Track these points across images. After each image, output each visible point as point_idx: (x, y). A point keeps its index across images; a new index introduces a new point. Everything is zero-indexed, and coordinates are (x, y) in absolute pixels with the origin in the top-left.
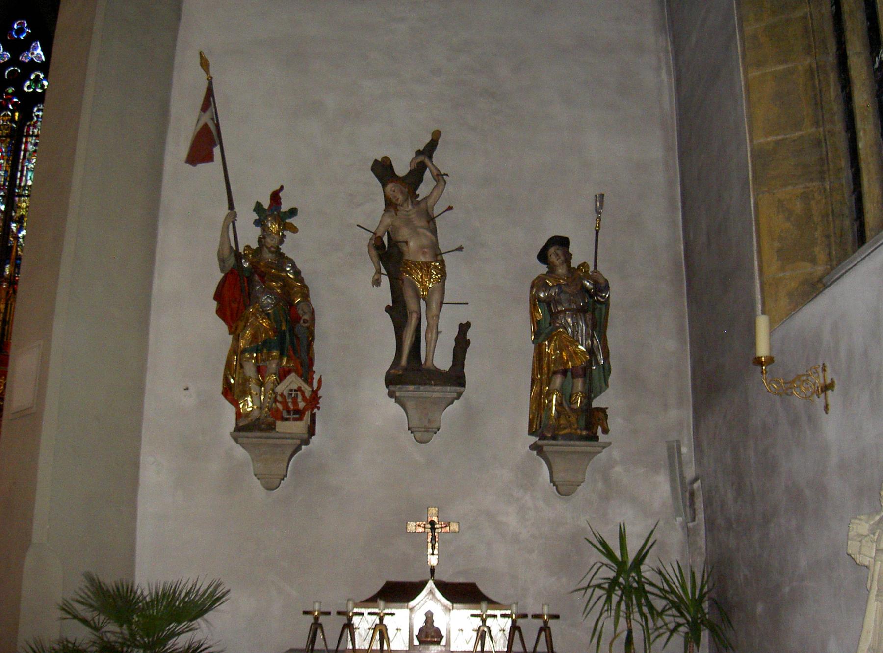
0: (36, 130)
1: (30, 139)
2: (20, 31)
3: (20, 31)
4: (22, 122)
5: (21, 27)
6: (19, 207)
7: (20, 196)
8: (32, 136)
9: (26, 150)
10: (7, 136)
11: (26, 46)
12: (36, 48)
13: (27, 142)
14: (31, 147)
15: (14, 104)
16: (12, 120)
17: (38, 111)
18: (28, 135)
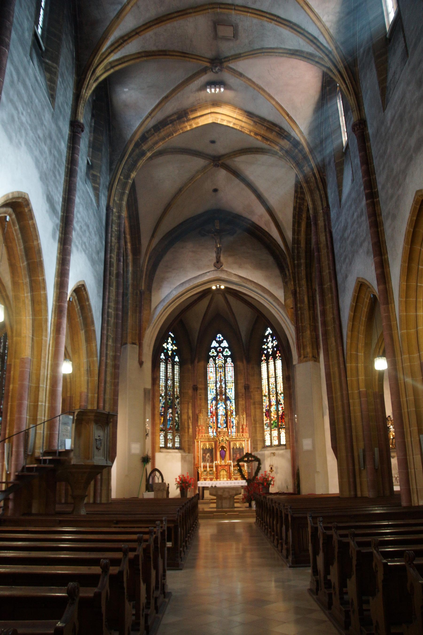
2: (219, 338)
3: (219, 338)
4: (225, 364)
5: (220, 336)
11: (221, 342)
14: (228, 370)
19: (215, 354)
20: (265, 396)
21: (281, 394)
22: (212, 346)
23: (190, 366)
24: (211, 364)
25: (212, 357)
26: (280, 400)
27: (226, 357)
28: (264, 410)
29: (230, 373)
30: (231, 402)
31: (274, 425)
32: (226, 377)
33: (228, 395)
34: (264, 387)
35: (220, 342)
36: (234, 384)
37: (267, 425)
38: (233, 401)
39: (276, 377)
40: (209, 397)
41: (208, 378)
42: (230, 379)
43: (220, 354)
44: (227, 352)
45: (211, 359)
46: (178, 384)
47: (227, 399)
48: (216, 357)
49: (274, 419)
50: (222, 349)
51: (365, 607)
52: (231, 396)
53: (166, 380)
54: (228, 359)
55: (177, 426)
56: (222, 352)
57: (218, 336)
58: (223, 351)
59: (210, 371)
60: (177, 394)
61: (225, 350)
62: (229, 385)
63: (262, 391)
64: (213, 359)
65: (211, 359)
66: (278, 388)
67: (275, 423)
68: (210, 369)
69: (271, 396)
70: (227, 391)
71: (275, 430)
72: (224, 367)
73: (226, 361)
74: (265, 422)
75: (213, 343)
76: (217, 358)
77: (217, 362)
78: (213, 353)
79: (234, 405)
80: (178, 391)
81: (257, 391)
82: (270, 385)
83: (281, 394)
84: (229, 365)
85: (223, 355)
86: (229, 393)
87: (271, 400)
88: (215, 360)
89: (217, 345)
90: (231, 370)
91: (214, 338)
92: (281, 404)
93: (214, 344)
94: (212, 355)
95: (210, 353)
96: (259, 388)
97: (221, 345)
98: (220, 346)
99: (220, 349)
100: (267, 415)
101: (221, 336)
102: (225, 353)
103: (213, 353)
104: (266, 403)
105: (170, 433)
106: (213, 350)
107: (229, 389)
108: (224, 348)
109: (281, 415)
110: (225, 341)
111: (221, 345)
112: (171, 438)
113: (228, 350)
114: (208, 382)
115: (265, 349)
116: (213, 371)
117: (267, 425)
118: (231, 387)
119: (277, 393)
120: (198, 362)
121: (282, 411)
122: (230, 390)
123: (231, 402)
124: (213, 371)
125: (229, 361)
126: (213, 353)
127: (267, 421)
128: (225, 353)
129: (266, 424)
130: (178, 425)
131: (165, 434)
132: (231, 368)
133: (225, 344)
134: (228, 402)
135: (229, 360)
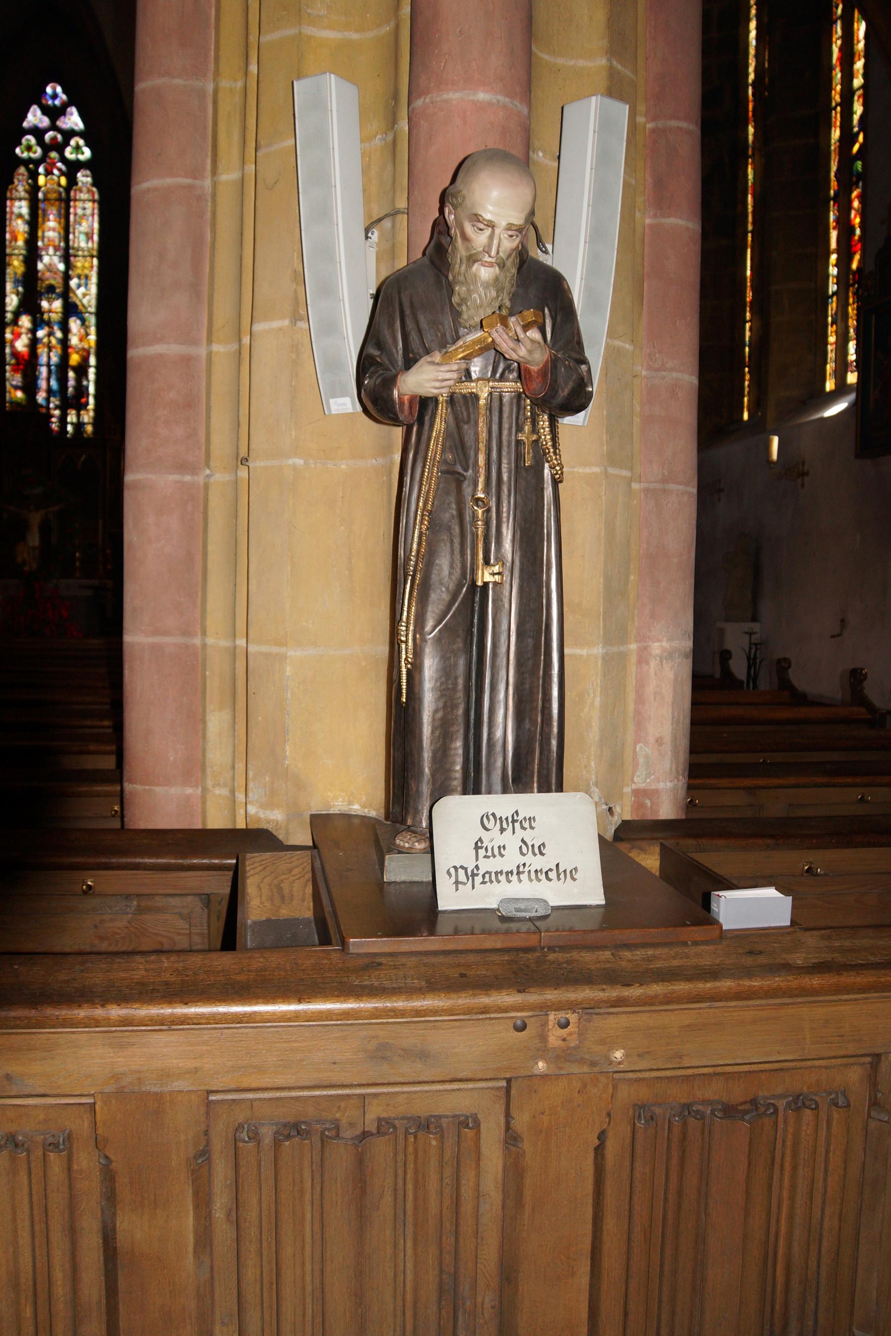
1: (77, 203)
3: (55, 96)
4: (68, 189)
5: (55, 91)
6: (75, 267)
7: (75, 256)
8: (80, 200)
9: (75, 214)
10: (56, 200)
12: (72, 114)
13: (75, 207)
14: (80, 212)
15: (60, 170)
16: (59, 185)
17: (83, 176)
18: (75, 200)
19: (38, 152)
22: (25, 124)
24: (20, 188)
25: (26, 162)
27: (73, 167)
29: (84, 224)
30: (83, 321)
32: (71, 236)
33: (73, 299)
35: (55, 113)
36: (95, 261)
38: (92, 320)
40: (8, 300)
41: (8, 236)
42: (83, 244)
43: (54, 155)
45: (22, 170)
47: (71, 309)
48: (37, 163)
50: (59, 137)
51: (502, 878)
52: (85, 301)
54: (79, 175)
56: (60, 148)
57: (49, 90)
58: (66, 143)
59: (16, 210)
61: (73, 142)
62: (79, 264)
64: (28, 169)
65: (22, 170)
68: (17, 204)
70: (73, 283)
72: (65, 201)
73: (72, 181)
75: (30, 116)
76: (41, 170)
77: (42, 180)
78: (28, 149)
79: (93, 330)
84: (84, 196)
85: (63, 160)
86: (80, 292)
88: (34, 175)
89: (45, 122)
90: (89, 212)
91: (37, 97)
93: (35, 117)
94: (25, 155)
95: (18, 151)
97: (60, 123)
98: (54, 127)
99: (54, 139)
101: (59, 89)
102: (69, 153)
103: (29, 148)
106: (31, 139)
107: (79, 277)
108: (69, 134)
110: (73, 110)
111: (60, 123)
113: (81, 142)
114: (8, 251)
118: (86, 272)
122: (83, 281)
123: (83, 321)
125: (85, 179)
126: (29, 148)
128: (69, 153)
132: (89, 205)
133: (74, 120)
134: (74, 324)
135: (84, 178)
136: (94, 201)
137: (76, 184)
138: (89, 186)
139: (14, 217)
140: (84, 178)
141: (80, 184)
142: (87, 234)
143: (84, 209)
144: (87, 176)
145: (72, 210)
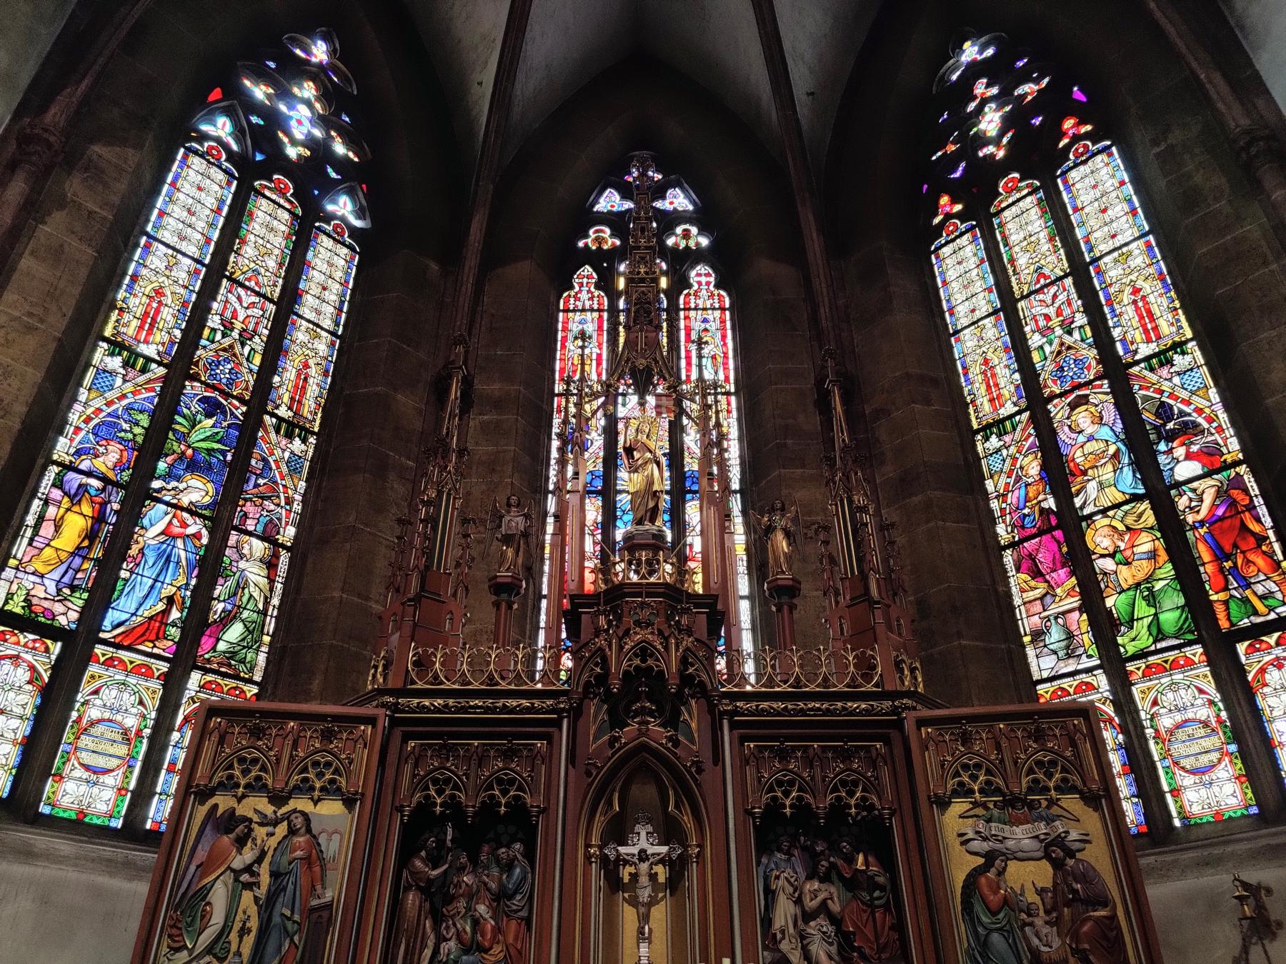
0: (700, 302)
1: (692, 314)
17: (699, 275)
18: (687, 309)
20: (998, 426)
21: (1162, 359)
23: (434, 266)
24: (584, 296)
26: (1164, 411)
28: (1002, 532)
31: (1141, 627)
34: (975, 371)
37: (1055, 636)
39: (1081, 270)
44: (686, 235)
45: (587, 270)
46: (322, 348)
49: (1126, 575)
53: (216, 272)
55: (235, 632)
59: (575, 328)
60: (296, 403)
63: (959, 404)
66: (1125, 327)
67: (1152, 599)
68: (578, 316)
69: (1057, 410)
71: (1175, 665)
73: (680, 283)
74: (1028, 623)
80: (313, 390)
81: (928, 402)
82: (1035, 340)
83: (1162, 359)
87: (1064, 435)
90: (713, 326)
92: (1188, 430)
96: (935, 382)
100: (1043, 558)
103: (599, 240)
104: (1009, 471)
105: (148, 673)
109: (1212, 521)
112: (131, 722)
115: (950, 162)
116: (590, 328)
117: (1055, 636)
119: (1115, 370)
120: (492, 260)
121: (1208, 488)
124: (590, 328)
125: (703, 279)
127: (1054, 609)
129: (1038, 635)
130: (253, 631)
131: (56, 668)
135: (701, 276)
136: (723, 309)
137: (690, 286)
138: (711, 287)
139: (570, 337)
140: (701, 276)
141: (696, 287)
142: (714, 357)
143: (705, 321)
144: (708, 275)
145: (682, 324)
